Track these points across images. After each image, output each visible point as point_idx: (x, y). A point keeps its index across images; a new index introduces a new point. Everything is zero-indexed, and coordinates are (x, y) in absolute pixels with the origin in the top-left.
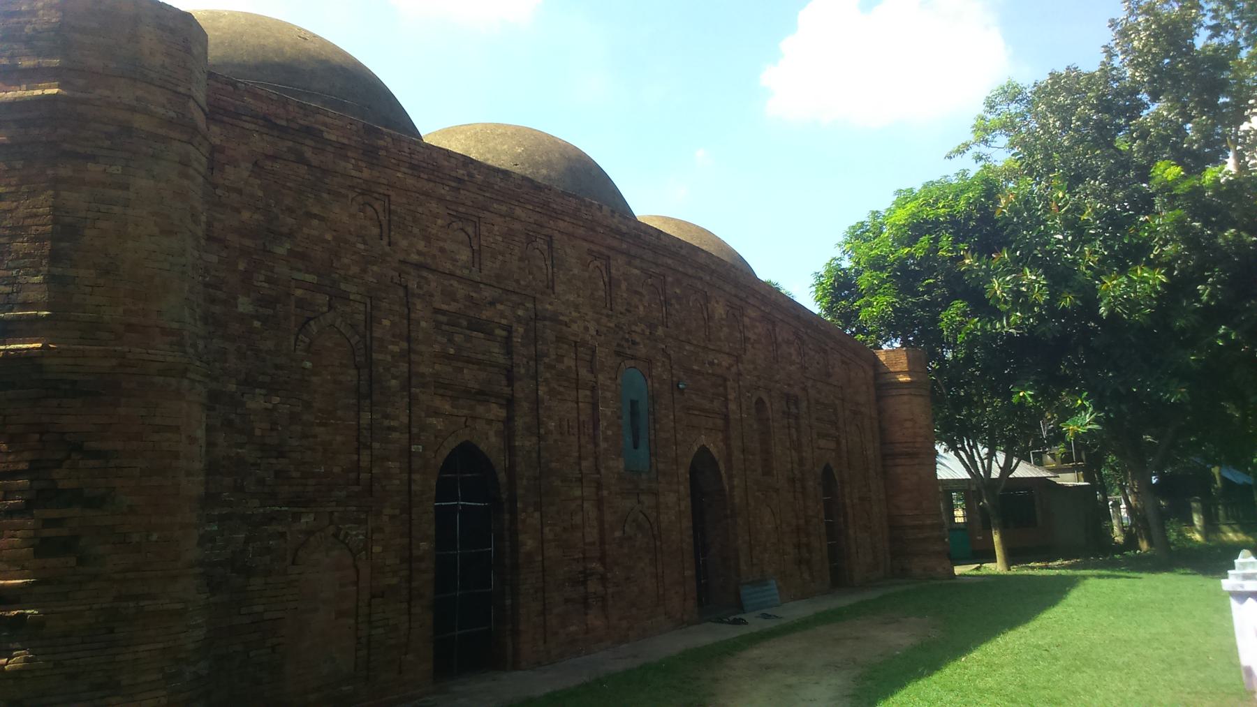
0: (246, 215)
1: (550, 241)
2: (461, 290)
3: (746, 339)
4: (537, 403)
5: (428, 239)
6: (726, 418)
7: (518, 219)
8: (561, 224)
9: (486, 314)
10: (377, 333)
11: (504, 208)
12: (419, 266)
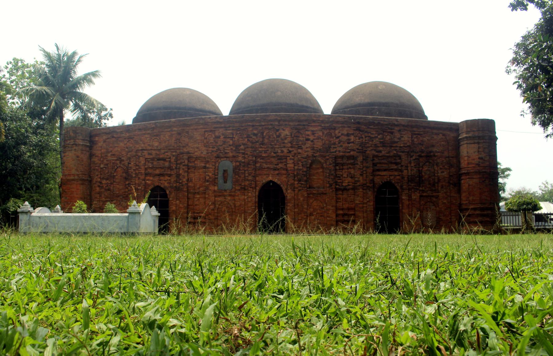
0: (102, 151)
1: (188, 132)
2: (154, 152)
3: (308, 140)
4: (178, 175)
5: (144, 144)
6: (287, 170)
7: (175, 131)
8: (192, 127)
9: (161, 157)
10: (130, 166)
11: (169, 130)
12: (142, 150)
